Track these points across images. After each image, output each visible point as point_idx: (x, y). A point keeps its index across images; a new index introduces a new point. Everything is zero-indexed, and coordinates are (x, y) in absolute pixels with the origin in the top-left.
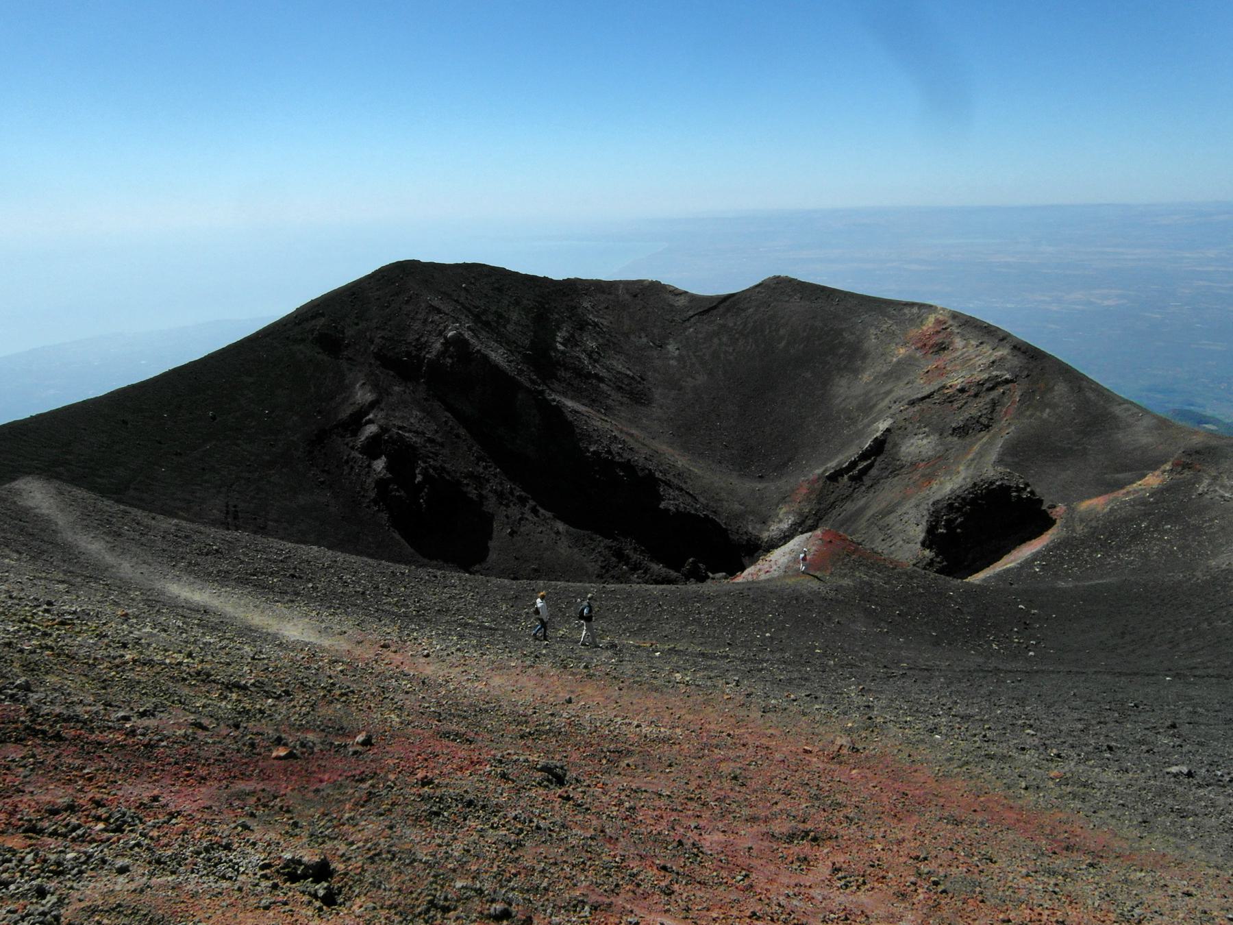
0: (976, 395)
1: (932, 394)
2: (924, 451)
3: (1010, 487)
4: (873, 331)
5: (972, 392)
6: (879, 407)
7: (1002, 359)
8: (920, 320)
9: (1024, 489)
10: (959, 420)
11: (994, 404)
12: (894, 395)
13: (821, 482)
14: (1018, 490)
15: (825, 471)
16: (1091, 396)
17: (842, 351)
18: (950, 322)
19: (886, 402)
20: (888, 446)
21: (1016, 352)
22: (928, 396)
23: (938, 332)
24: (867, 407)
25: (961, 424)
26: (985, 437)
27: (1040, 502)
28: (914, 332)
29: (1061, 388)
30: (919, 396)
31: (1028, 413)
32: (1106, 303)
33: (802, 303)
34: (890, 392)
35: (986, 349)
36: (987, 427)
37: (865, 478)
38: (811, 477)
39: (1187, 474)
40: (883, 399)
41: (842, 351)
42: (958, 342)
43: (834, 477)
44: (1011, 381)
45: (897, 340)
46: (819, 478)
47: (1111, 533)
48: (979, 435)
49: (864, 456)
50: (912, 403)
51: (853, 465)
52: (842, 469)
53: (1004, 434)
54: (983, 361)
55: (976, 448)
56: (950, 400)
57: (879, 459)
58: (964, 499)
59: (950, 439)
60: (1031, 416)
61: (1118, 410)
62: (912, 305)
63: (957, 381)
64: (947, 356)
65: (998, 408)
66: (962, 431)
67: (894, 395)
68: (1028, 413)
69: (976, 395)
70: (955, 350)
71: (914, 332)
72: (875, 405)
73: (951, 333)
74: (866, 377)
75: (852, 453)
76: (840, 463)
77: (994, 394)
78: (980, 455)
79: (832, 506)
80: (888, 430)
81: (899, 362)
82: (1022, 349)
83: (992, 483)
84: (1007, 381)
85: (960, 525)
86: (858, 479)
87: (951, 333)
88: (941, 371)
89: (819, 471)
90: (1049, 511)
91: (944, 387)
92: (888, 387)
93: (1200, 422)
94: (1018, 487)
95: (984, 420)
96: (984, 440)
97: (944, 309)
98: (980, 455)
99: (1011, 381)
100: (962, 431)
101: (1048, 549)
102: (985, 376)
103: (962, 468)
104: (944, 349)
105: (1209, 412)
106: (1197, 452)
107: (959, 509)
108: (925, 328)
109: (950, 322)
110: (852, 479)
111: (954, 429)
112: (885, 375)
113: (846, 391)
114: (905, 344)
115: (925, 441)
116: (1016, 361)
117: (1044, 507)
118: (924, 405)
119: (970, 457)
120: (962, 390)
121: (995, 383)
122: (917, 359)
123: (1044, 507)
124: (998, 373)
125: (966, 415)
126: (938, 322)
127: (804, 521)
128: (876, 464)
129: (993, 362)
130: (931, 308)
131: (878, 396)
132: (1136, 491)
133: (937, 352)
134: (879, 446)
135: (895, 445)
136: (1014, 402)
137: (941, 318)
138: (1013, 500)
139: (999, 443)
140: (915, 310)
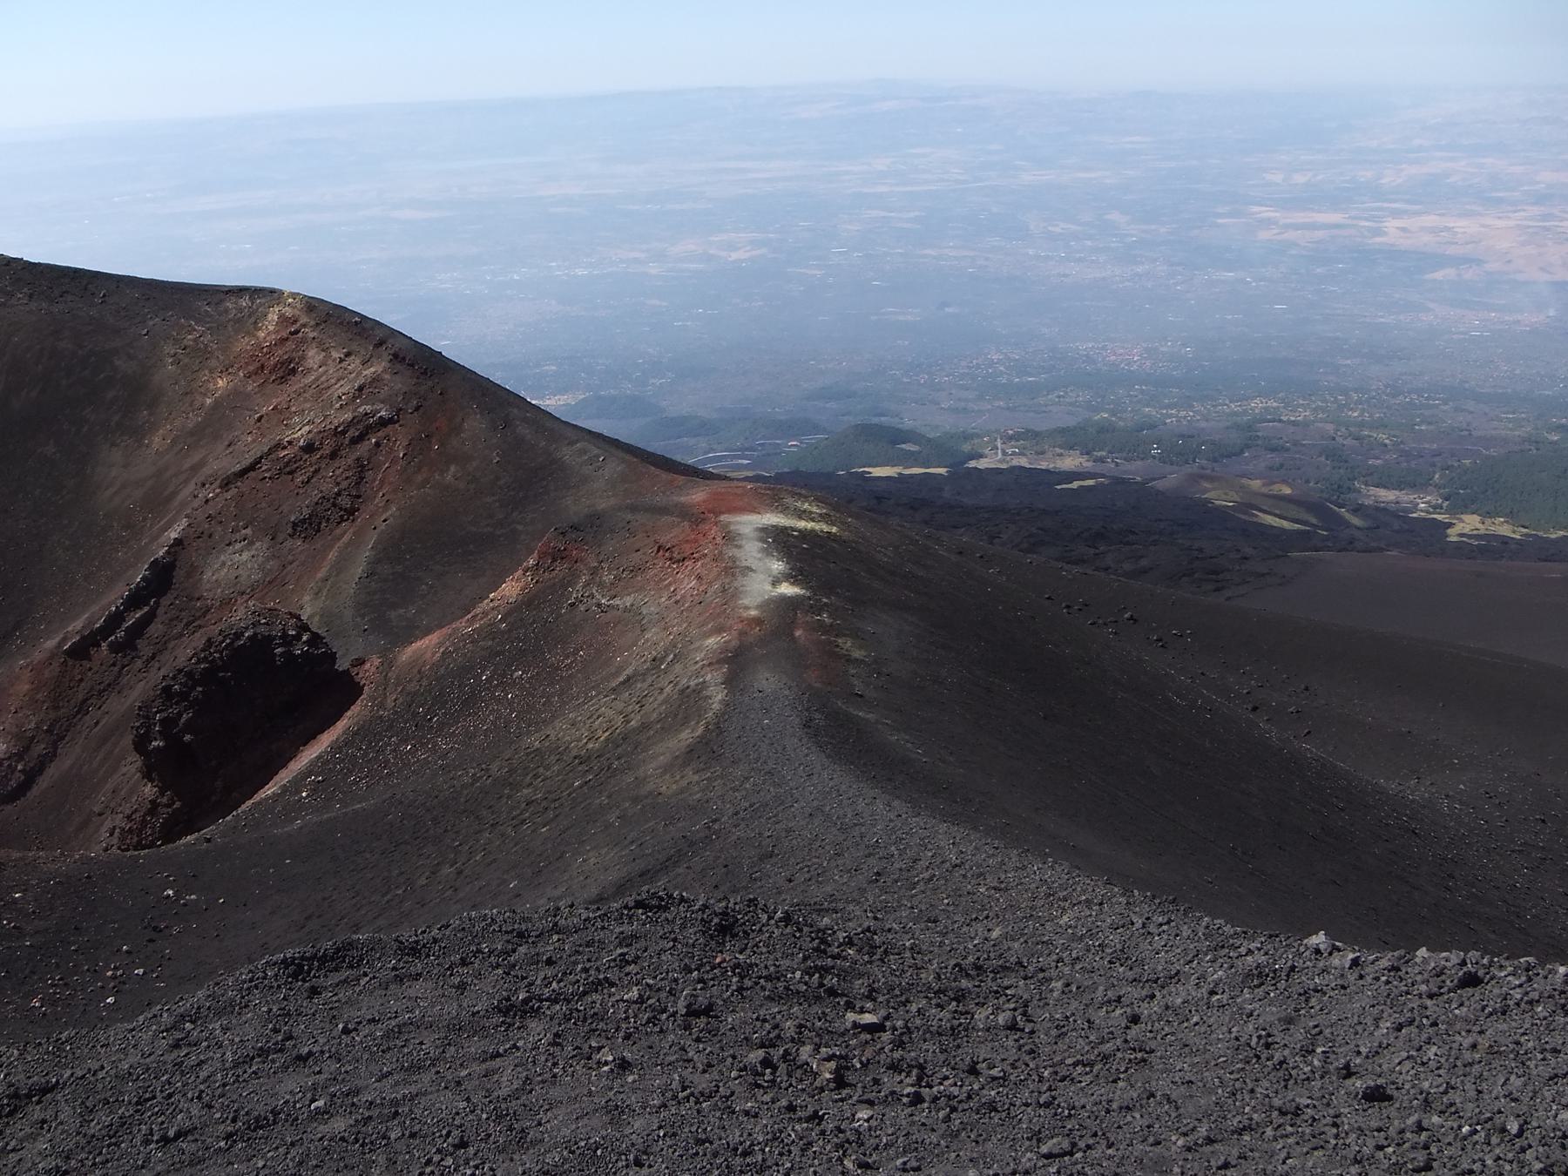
0: (334, 455)
1: (258, 461)
2: (243, 573)
3: (270, 639)
4: (169, 349)
5: (327, 450)
6: (180, 498)
7: (376, 380)
8: (256, 318)
9: (298, 637)
10: (299, 508)
11: (361, 468)
12: (207, 471)
13: (55, 664)
14: (287, 641)
15: (64, 640)
16: (524, 430)
17: (110, 395)
18: (304, 319)
19: (191, 487)
20: (179, 574)
21: (398, 367)
22: (252, 467)
23: (284, 340)
24: (157, 502)
25: (306, 512)
26: (347, 532)
27: (331, 657)
28: (244, 344)
29: (475, 424)
30: (238, 468)
31: (419, 478)
32: (734, 256)
33: (33, 305)
34: (195, 469)
35: (354, 363)
36: (351, 512)
37: (140, 643)
38: (38, 656)
39: (561, 569)
40: (186, 481)
41: (110, 395)
42: (313, 356)
43: (82, 650)
44: (391, 421)
45: (213, 363)
46: (53, 655)
47: (447, 695)
48: (338, 532)
49: (135, 600)
50: (226, 484)
51: (115, 620)
52: (93, 634)
53: (379, 521)
54: (345, 388)
55: (332, 555)
56: (288, 469)
57: (165, 601)
58: (190, 675)
59: (289, 543)
60: (426, 481)
61: (567, 454)
62: (240, 291)
63: (300, 433)
64: (297, 383)
65: (369, 475)
66: (310, 527)
67: (207, 471)
68: (419, 478)
69: (334, 455)
70: (309, 370)
71: (244, 344)
72: (174, 494)
73: (303, 341)
74: (157, 441)
75: (114, 598)
76: (91, 622)
77: (363, 449)
78: (339, 567)
79: (82, 709)
80: (178, 542)
81: (217, 405)
82: (422, 364)
83: (238, 635)
84: (384, 423)
85: (188, 728)
86: (126, 647)
87: (303, 341)
88: (282, 414)
89: (51, 644)
90: (354, 671)
91: (279, 446)
92: (196, 457)
93: (894, 443)
94: (285, 635)
95: (345, 501)
96: (346, 539)
97: (294, 295)
98: (339, 567)
99: (391, 421)
100: (310, 527)
101: (336, 747)
102: (348, 416)
103: (307, 598)
104: (293, 371)
105: (908, 424)
106: (574, 528)
107: (183, 696)
108: (261, 334)
109: (304, 319)
110: (116, 648)
111: (295, 525)
112: (192, 434)
113: (121, 471)
114: (225, 370)
115: (245, 556)
116: (398, 384)
117: (342, 664)
118: (243, 486)
119: (320, 575)
120: (309, 448)
121: (363, 429)
122: (248, 396)
123: (342, 664)
124: (368, 408)
125: (315, 495)
126: (283, 319)
127: (27, 749)
128: (160, 611)
129: (361, 389)
130: (273, 295)
131: (168, 475)
132: (485, 614)
133: (283, 380)
134: (163, 576)
135: (194, 571)
136: (394, 461)
137: (288, 312)
138: (279, 661)
139: (372, 539)
140: (244, 302)
